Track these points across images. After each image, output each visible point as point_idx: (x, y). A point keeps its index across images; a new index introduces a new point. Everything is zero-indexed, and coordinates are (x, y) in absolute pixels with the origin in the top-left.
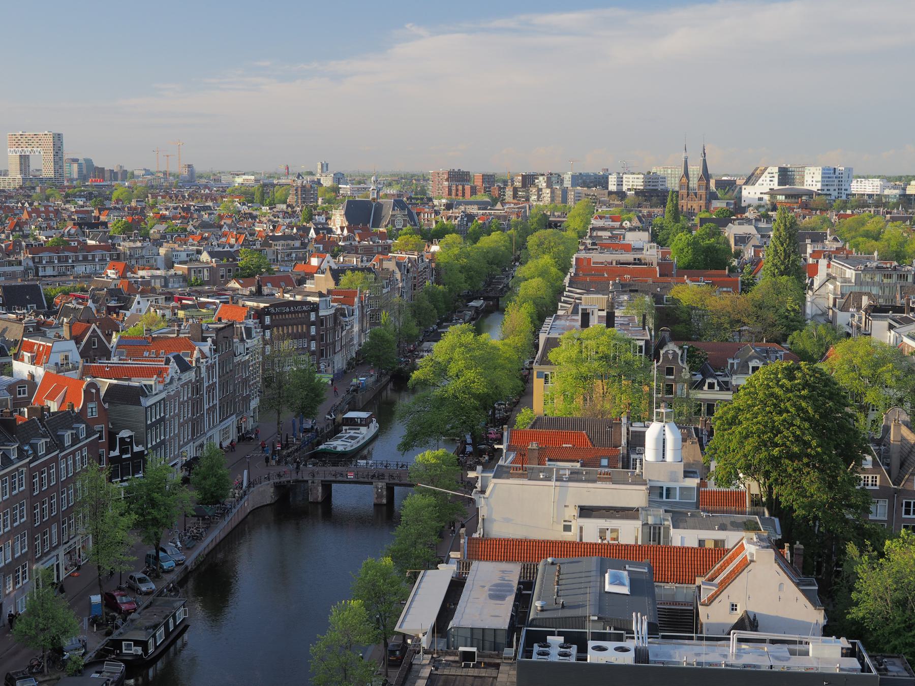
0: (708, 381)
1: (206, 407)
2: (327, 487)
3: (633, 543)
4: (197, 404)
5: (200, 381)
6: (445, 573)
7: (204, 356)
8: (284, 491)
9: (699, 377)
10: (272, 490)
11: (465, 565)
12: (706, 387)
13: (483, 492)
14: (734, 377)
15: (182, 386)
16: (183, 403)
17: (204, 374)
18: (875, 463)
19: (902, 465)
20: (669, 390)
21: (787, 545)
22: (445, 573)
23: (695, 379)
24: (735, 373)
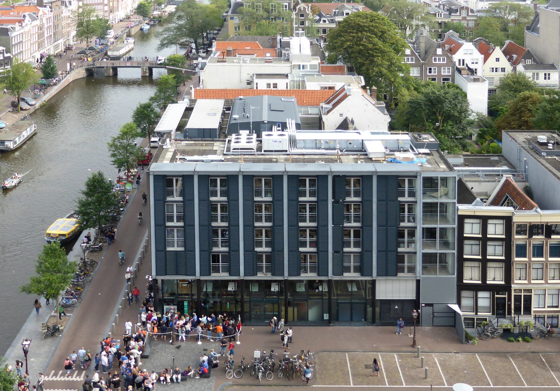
0: (322, 19)
1: (46, 36)
2: (115, 69)
3: (285, 89)
4: (41, 35)
5: (43, 25)
6: (182, 105)
7: (45, 14)
8: (90, 72)
9: (318, 18)
10: (84, 71)
11: (193, 102)
12: (322, 22)
13: (202, 69)
14: (336, 17)
15: (33, 27)
16: (33, 34)
17: (44, 21)
18: (412, 52)
19: (426, 53)
20: (303, 23)
21: (368, 88)
22: (182, 105)
23: (315, 18)
24: (337, 15)
